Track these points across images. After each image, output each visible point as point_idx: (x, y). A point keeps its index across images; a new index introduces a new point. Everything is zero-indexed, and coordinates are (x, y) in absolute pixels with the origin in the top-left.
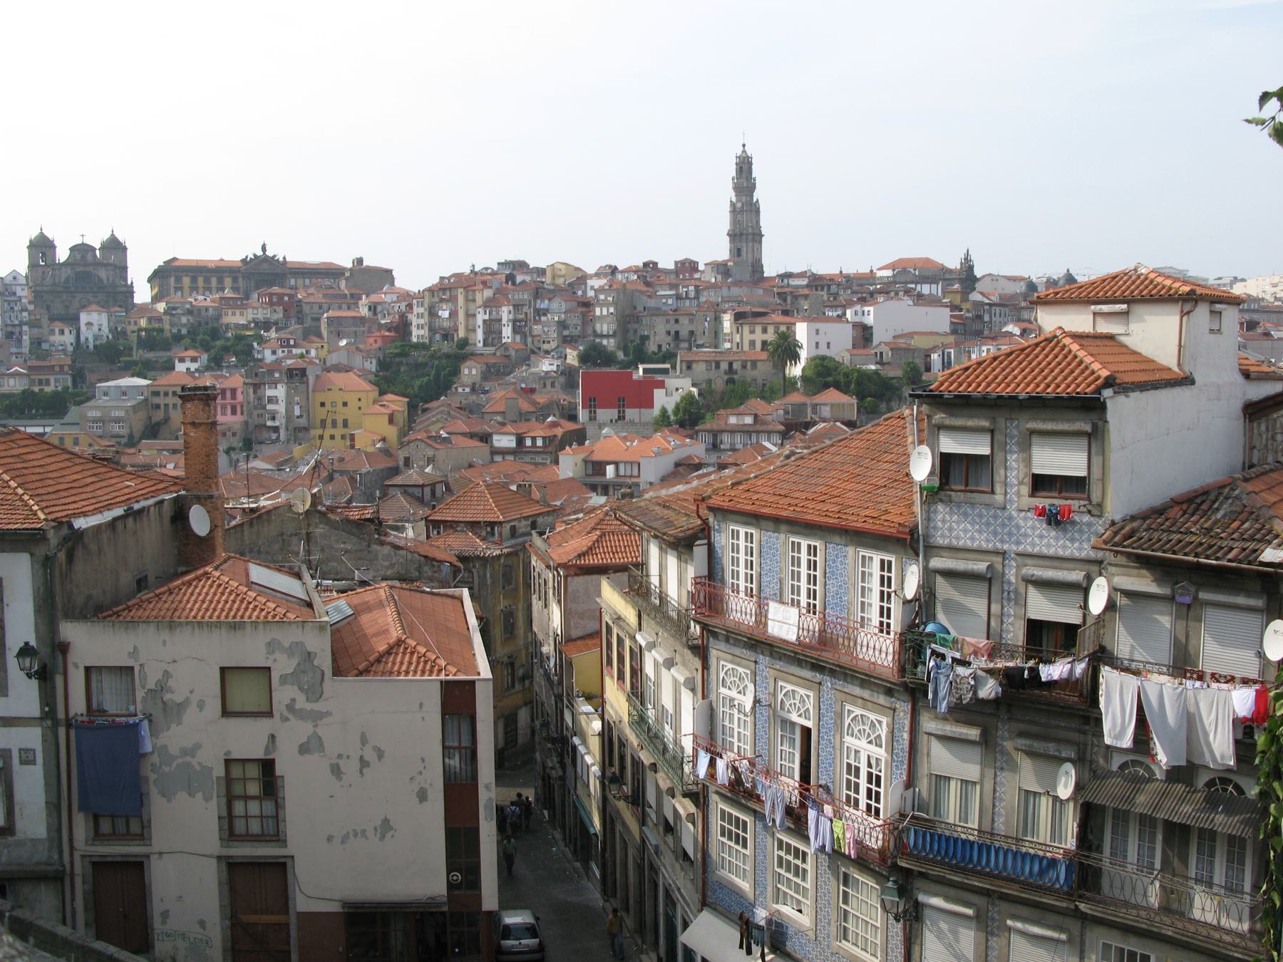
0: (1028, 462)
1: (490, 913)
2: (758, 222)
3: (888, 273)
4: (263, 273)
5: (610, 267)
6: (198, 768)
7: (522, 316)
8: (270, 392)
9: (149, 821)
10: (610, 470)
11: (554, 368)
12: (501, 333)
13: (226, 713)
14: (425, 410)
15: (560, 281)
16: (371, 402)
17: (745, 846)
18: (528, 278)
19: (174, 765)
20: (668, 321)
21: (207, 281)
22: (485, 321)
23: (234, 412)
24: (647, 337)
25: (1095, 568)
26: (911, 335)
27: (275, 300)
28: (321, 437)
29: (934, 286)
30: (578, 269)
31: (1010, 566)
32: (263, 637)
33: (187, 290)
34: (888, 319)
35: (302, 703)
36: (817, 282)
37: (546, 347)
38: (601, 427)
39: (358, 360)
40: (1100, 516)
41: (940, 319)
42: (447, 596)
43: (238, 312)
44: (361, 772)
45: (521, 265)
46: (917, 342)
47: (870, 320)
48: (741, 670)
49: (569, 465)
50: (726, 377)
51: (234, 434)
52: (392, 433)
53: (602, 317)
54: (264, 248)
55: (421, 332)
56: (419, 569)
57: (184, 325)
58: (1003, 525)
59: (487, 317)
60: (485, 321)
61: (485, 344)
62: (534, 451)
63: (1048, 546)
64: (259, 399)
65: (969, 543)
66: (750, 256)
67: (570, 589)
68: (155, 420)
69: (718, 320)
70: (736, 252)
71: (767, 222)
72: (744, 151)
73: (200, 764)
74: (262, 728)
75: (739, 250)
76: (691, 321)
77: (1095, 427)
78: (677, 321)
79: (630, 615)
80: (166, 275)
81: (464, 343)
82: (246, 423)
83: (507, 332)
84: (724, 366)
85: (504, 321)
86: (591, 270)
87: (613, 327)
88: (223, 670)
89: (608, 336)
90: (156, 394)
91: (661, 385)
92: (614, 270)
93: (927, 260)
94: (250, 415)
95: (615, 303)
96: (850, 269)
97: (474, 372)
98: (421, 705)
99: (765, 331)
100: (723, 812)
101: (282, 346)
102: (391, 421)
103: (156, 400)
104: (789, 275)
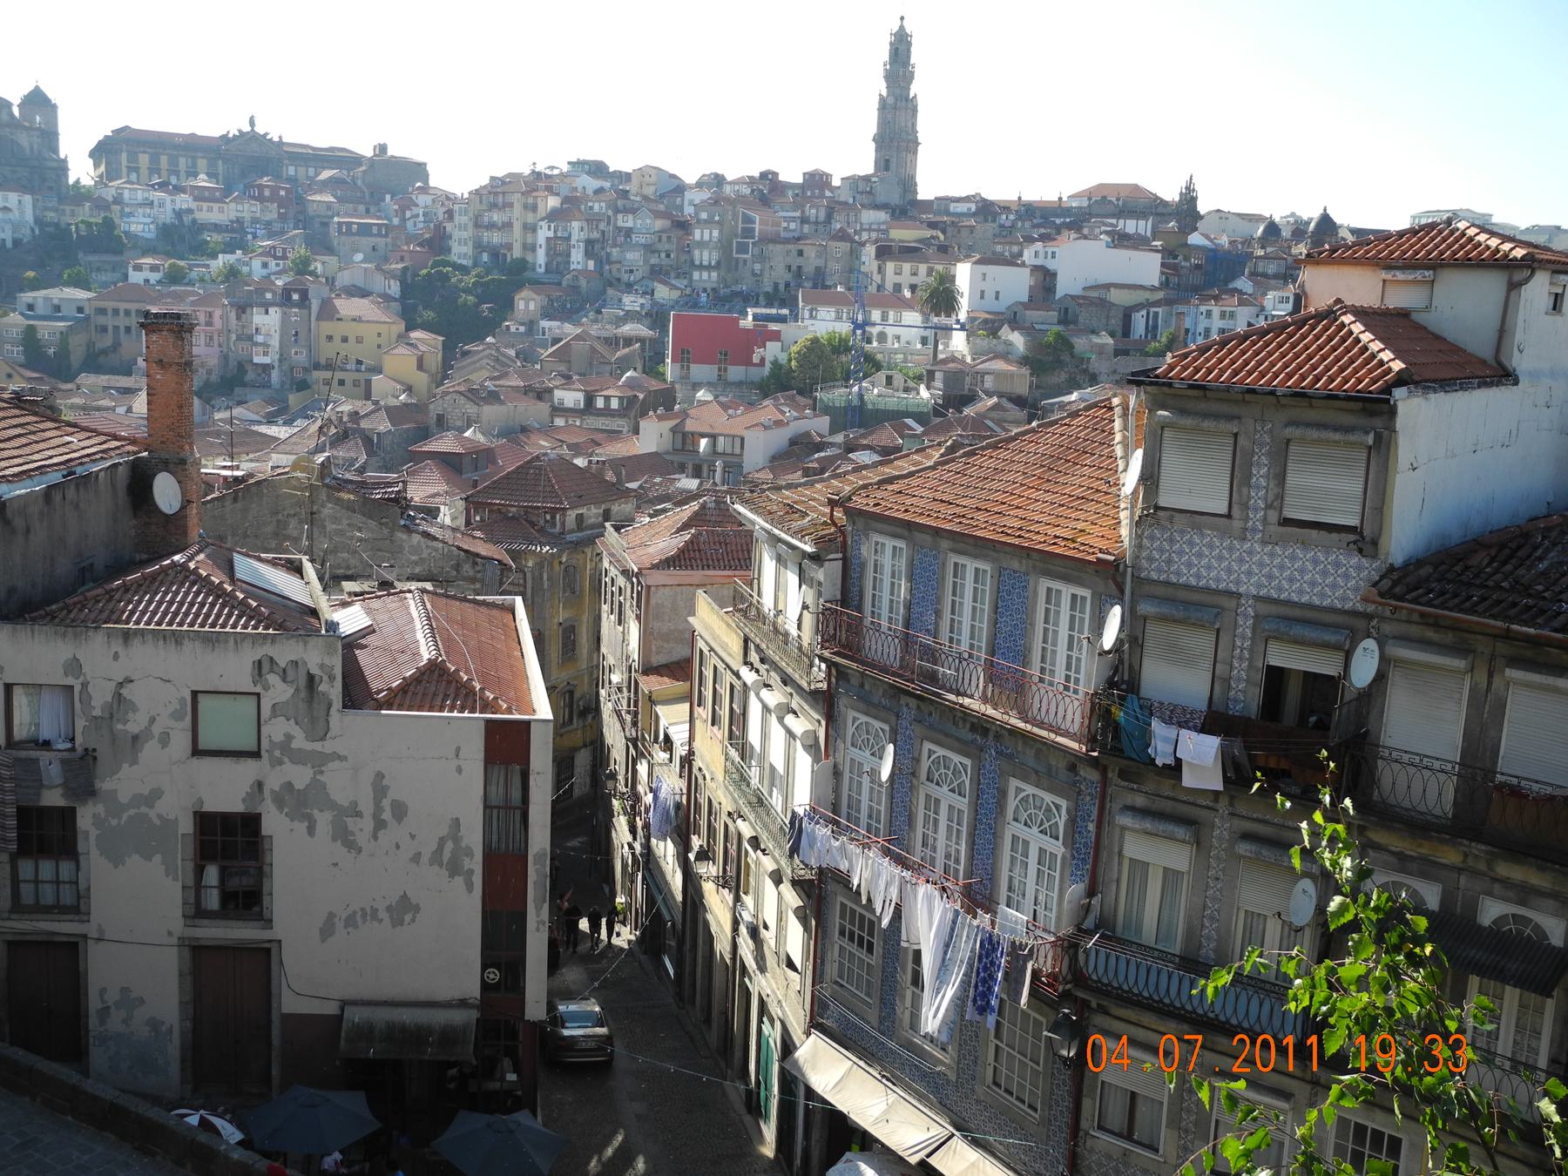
0: (1281, 478)
1: (538, 1025)
2: (914, 125)
3: (1085, 203)
5: (717, 176)
6: (157, 822)
7: (595, 235)
8: (258, 318)
9: (88, 889)
10: (703, 442)
12: (569, 255)
13: (197, 752)
14: (465, 354)
15: (649, 191)
16: (394, 337)
17: (870, 950)
18: (607, 185)
19: (125, 817)
20: (788, 252)
22: (548, 239)
25: (1360, 624)
26: (1108, 286)
27: (267, 193)
29: (1142, 223)
30: (674, 176)
31: (1246, 616)
32: (251, 654)
34: (1082, 263)
35: (300, 742)
36: (986, 209)
38: (696, 386)
39: (379, 283)
40: (1375, 556)
41: (1146, 268)
42: (493, 605)
43: (216, 206)
44: (375, 838)
45: (597, 169)
46: (1116, 296)
47: (1051, 265)
48: (877, 724)
49: (651, 436)
51: (209, 372)
52: (421, 380)
53: (702, 244)
54: (252, 122)
55: (464, 249)
56: (457, 567)
58: (1241, 561)
59: (551, 234)
60: (548, 239)
61: (547, 271)
62: (607, 412)
63: (1301, 592)
65: (1193, 582)
67: (653, 601)
68: (99, 345)
69: (855, 253)
70: (883, 164)
71: (925, 127)
72: (902, 27)
73: (160, 816)
74: (247, 771)
77: (1378, 438)
78: (800, 253)
79: (731, 644)
80: (117, 149)
81: (522, 266)
83: (577, 257)
85: (574, 238)
86: (690, 178)
88: (195, 694)
89: (709, 268)
90: (102, 311)
91: (776, 336)
92: (718, 180)
93: (1136, 187)
97: (532, 306)
98: (458, 750)
100: (843, 906)
101: (276, 258)
102: (420, 367)
103: (101, 320)
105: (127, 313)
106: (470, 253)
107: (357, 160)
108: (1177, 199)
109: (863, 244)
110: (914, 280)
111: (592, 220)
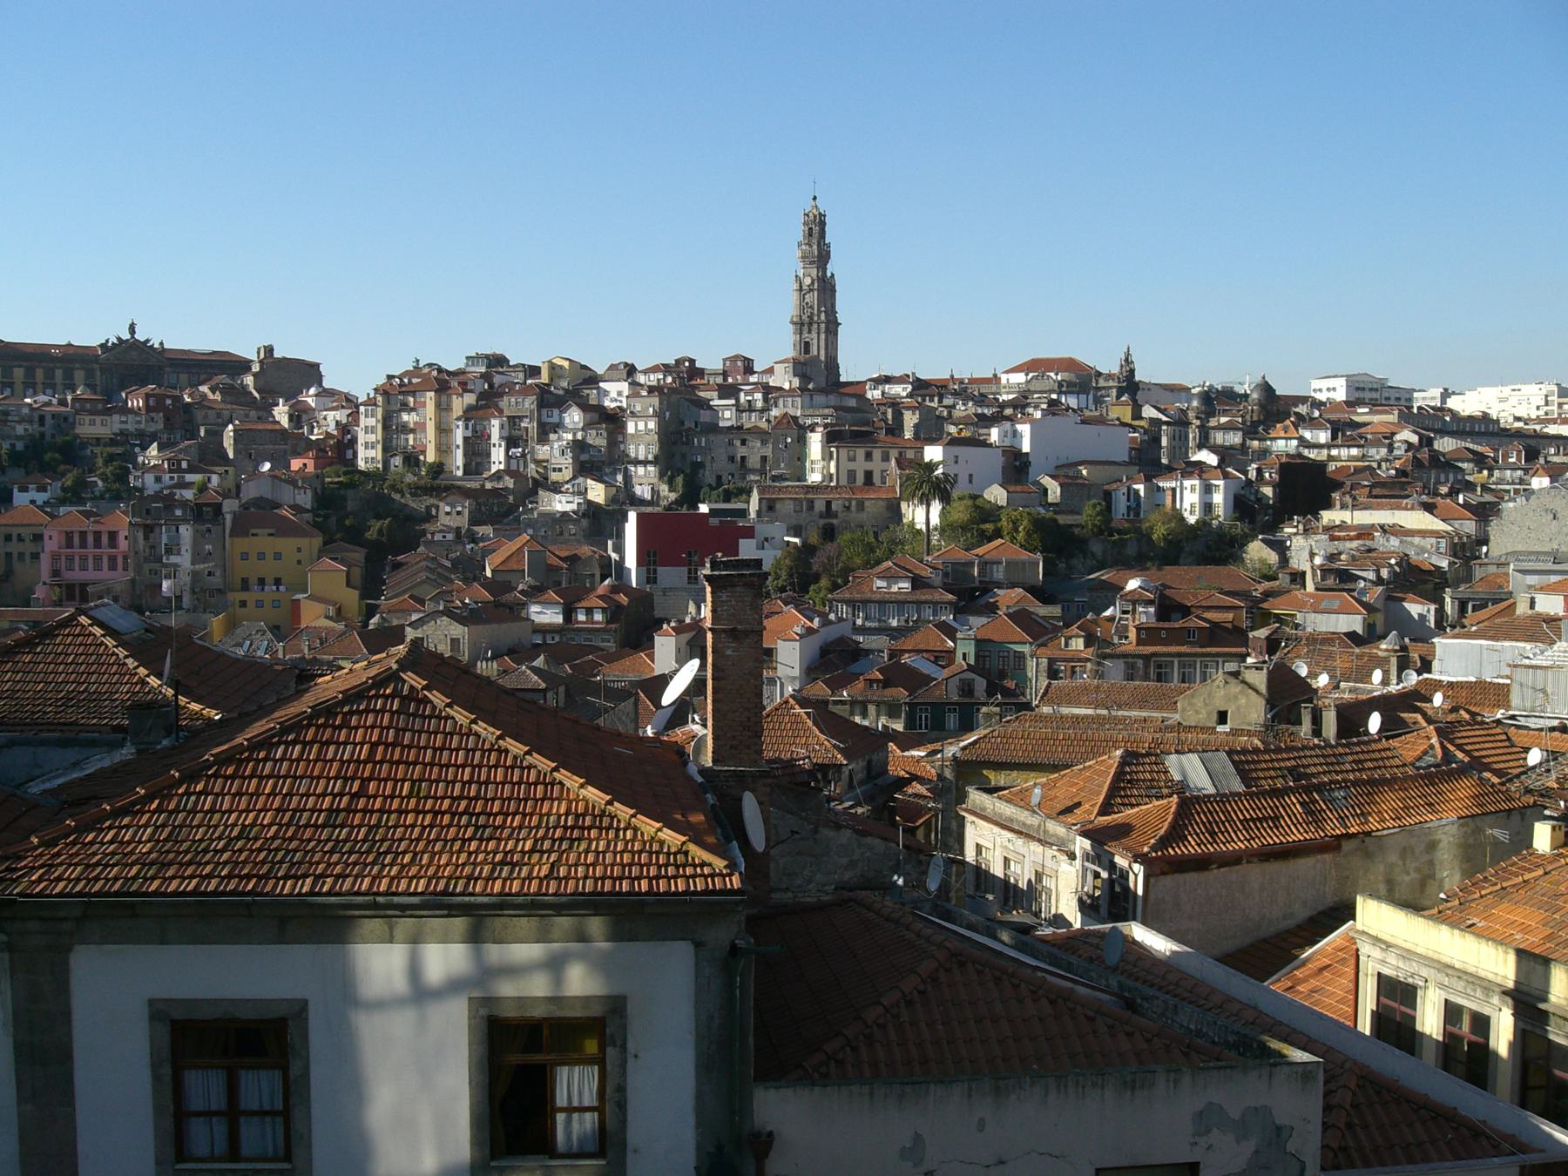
2: (833, 306)
3: (1019, 378)
4: (131, 362)
5: (626, 365)
11: (574, 506)
12: (489, 455)
14: (397, 566)
21: (50, 374)
23: (113, 567)
24: (701, 465)
28: (243, 604)
30: (584, 367)
33: (19, 387)
37: (554, 476)
43: (98, 419)
45: (497, 361)
50: (822, 522)
55: (372, 453)
57: (18, 438)
60: (466, 439)
61: (465, 473)
64: (152, 547)
66: (822, 352)
69: (802, 441)
75: (807, 344)
76: (764, 443)
81: (438, 469)
82: (133, 581)
83: (498, 456)
84: (820, 506)
86: (600, 370)
87: (655, 449)
94: (138, 570)
95: (658, 415)
96: (963, 373)
99: (869, 456)
102: (348, 585)
104: (888, 380)
105: (20, 539)
106: (380, 457)
107: (243, 365)
108: (1115, 370)
109: (813, 431)
110: (869, 466)
111: (513, 421)
